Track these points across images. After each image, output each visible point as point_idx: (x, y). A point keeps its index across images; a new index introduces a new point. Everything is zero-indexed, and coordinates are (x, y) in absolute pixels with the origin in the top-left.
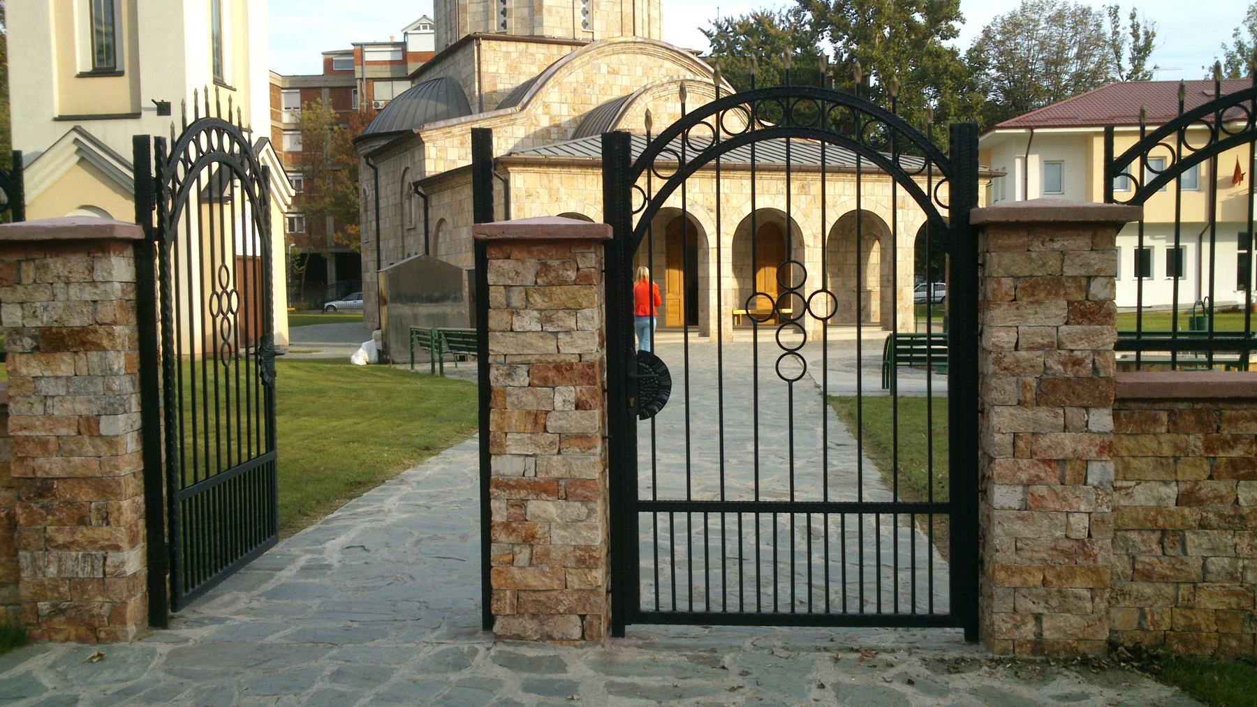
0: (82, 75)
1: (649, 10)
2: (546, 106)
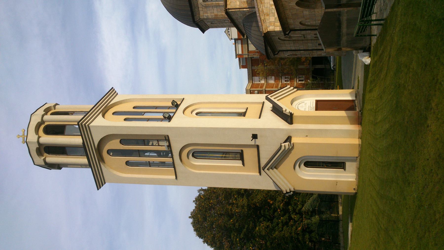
0: (243, 164)
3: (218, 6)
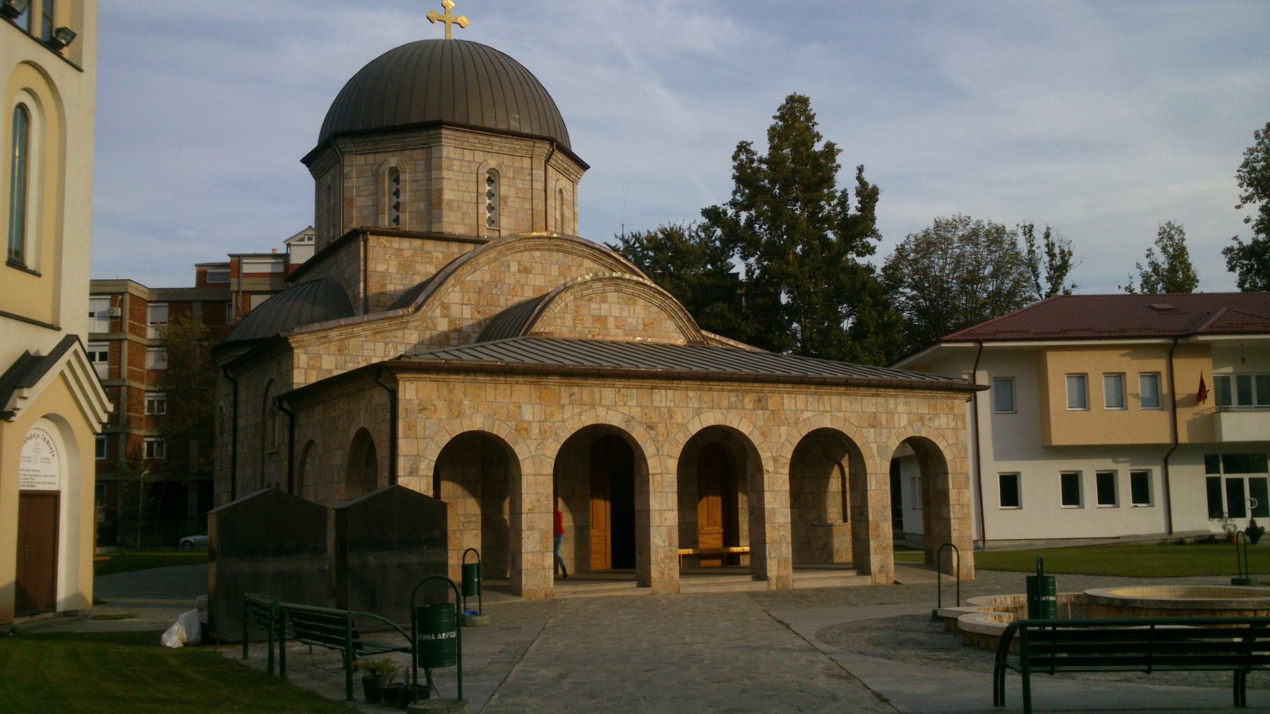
1: (562, 209)
2: (445, 307)
3: (377, 209)
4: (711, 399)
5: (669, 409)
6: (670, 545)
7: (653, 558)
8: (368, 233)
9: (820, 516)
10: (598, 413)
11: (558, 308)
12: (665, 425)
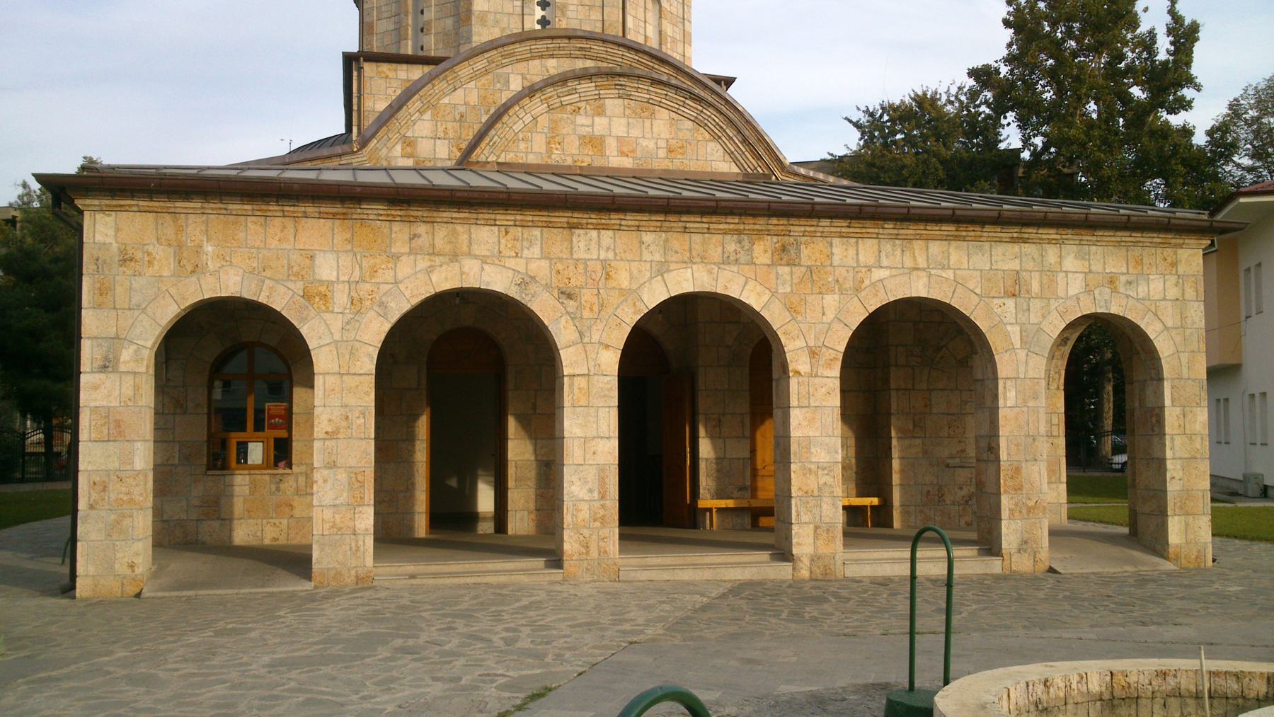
1: (660, 24)
2: (409, 143)
4: (687, 247)
5: (605, 263)
6: (603, 498)
7: (568, 519)
8: (362, 59)
9: (963, 451)
10: (466, 269)
11: (519, 125)
12: (595, 291)
